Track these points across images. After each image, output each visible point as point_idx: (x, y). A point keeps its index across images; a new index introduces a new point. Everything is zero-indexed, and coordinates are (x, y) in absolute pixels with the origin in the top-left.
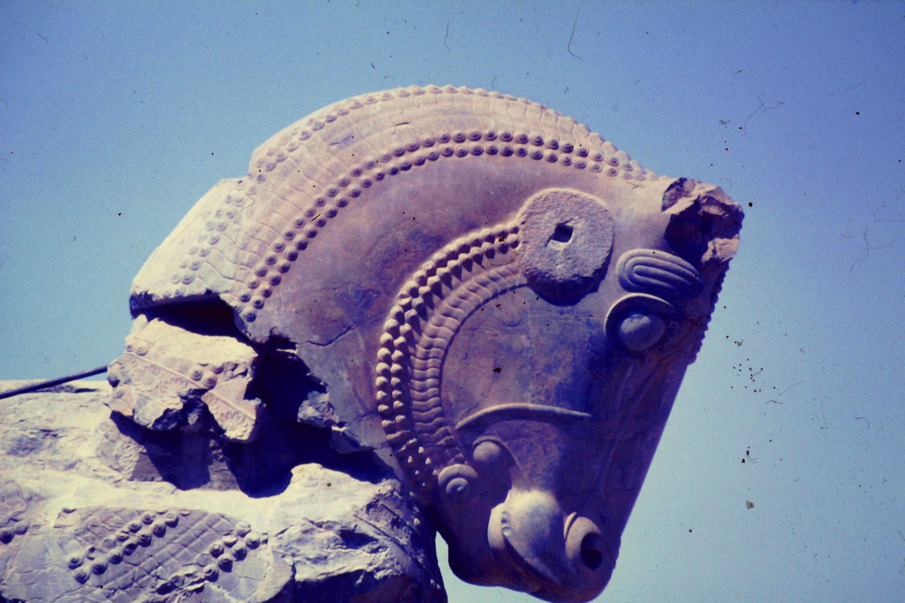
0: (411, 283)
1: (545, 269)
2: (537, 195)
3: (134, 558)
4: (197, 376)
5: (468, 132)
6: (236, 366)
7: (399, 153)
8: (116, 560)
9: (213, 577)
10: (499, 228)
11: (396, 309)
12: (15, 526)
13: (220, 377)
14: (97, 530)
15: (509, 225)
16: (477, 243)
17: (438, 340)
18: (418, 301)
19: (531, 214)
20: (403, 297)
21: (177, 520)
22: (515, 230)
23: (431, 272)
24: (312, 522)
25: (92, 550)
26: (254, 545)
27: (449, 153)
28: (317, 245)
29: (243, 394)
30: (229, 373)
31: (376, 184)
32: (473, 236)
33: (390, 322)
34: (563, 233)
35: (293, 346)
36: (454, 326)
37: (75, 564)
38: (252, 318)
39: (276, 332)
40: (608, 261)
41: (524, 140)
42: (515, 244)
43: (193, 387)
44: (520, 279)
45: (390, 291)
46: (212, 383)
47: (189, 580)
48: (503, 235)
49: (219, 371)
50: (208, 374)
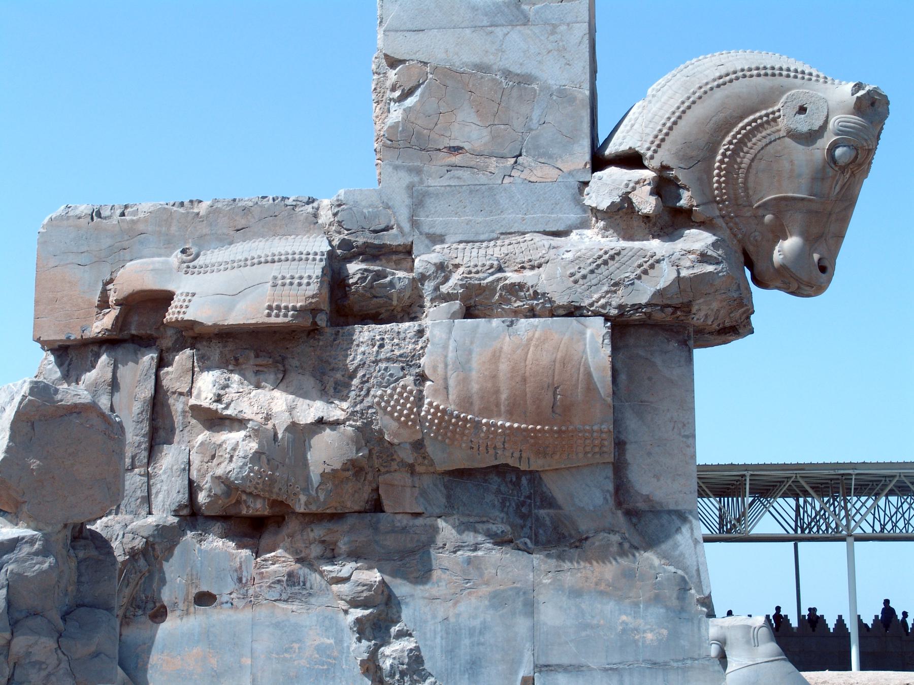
0: (728, 139)
1: (795, 127)
2: (789, 93)
3: (599, 271)
4: (627, 185)
5: (753, 66)
6: (645, 180)
7: (720, 77)
8: (592, 272)
9: (639, 278)
10: (770, 110)
11: (721, 151)
12: (543, 260)
13: (638, 186)
14: (581, 259)
15: (776, 108)
16: (761, 117)
17: (743, 165)
18: (732, 147)
19: (786, 102)
20: (724, 145)
21: (620, 251)
22: (779, 110)
23: (739, 133)
24: (685, 251)
25: (580, 268)
26: (658, 261)
27: (744, 76)
28: (681, 123)
29: (649, 194)
30: (642, 184)
31: (709, 93)
32: (758, 115)
33: (719, 157)
34: (802, 110)
35: (672, 169)
36: (751, 158)
37: (572, 275)
38: (652, 158)
39: (664, 164)
40: (826, 122)
41: (781, 69)
42: (779, 117)
43: (625, 191)
44: (783, 133)
45: (718, 143)
46: (634, 189)
47: (627, 280)
48: (773, 113)
49: (637, 183)
50: (632, 185)
